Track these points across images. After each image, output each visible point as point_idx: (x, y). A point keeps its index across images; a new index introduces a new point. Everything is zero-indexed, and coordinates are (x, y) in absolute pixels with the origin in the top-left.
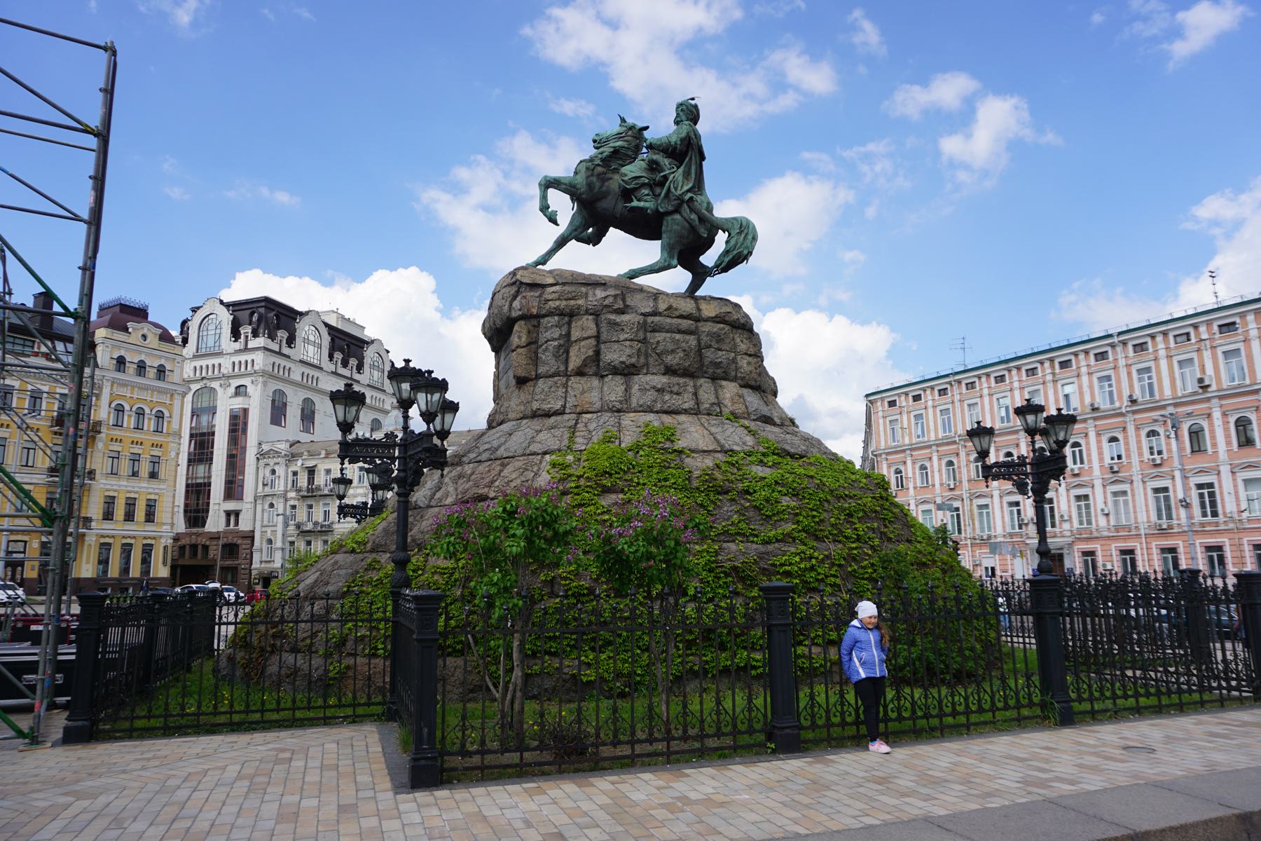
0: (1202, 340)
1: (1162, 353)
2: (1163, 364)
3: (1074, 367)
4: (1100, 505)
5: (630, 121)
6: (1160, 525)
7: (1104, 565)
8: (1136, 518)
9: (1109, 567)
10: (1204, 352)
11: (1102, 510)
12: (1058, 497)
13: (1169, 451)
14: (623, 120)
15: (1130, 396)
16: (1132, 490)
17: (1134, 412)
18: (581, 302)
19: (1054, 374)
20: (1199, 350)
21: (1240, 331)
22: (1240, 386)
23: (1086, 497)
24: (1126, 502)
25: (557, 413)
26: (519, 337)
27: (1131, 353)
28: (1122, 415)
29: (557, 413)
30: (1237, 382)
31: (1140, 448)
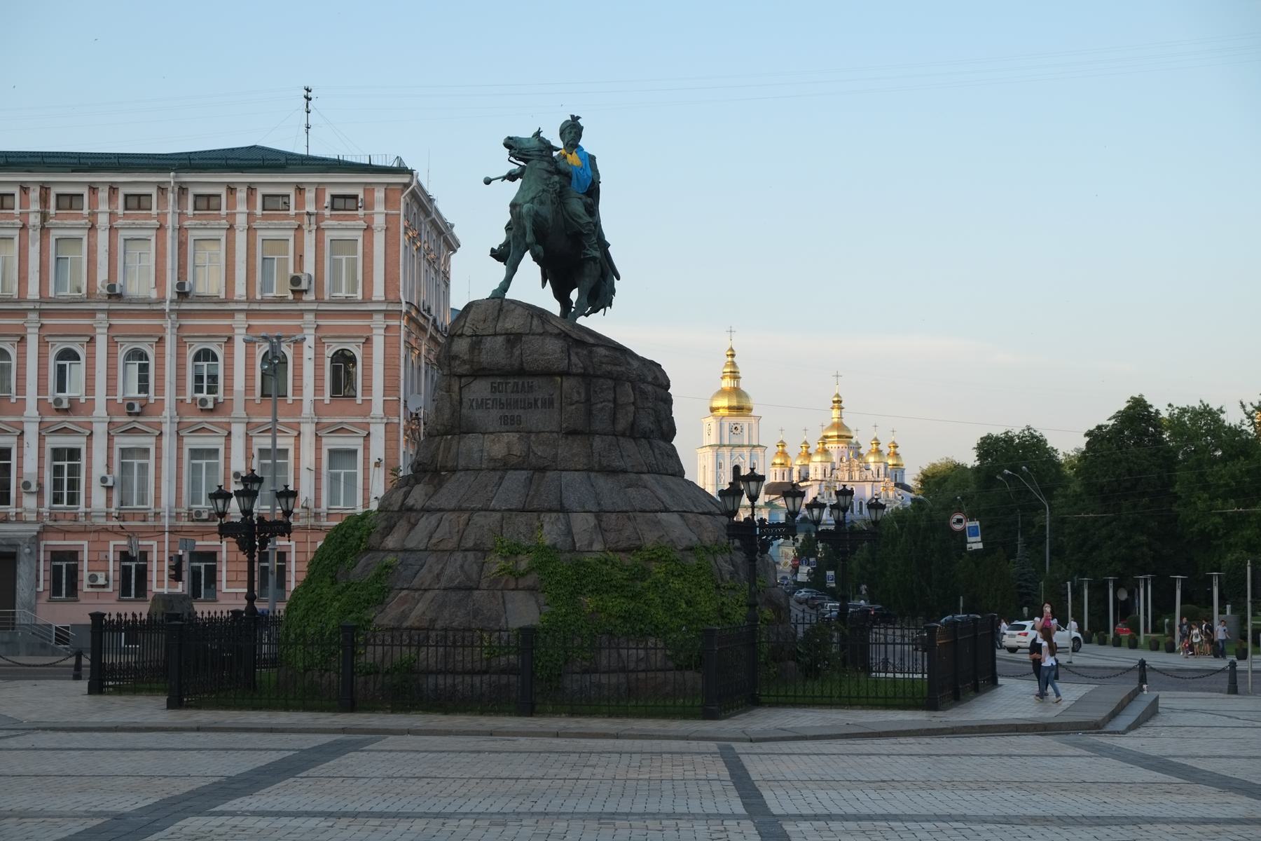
0: (308, 214)
1: (241, 221)
2: (241, 238)
3: (86, 211)
4: (99, 469)
5: (541, 135)
6: (199, 513)
7: (93, 578)
8: (158, 498)
9: (101, 581)
10: (306, 232)
11: (104, 480)
12: (20, 447)
13: (229, 389)
14: (539, 133)
15: (181, 285)
16: (158, 448)
17: (181, 314)
18: (623, 369)
19: (44, 216)
20: (299, 228)
21: (361, 212)
22: (347, 301)
23: (74, 454)
24: (143, 468)
25: (625, 471)
26: (578, 393)
27: (190, 211)
28: (161, 314)
29: (625, 471)
30: (343, 294)
31: (180, 377)
